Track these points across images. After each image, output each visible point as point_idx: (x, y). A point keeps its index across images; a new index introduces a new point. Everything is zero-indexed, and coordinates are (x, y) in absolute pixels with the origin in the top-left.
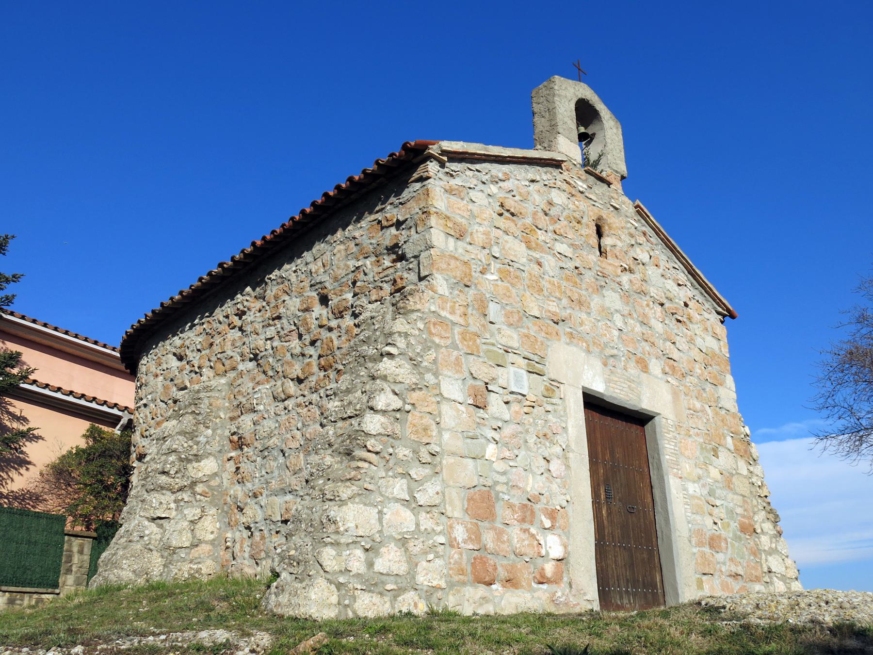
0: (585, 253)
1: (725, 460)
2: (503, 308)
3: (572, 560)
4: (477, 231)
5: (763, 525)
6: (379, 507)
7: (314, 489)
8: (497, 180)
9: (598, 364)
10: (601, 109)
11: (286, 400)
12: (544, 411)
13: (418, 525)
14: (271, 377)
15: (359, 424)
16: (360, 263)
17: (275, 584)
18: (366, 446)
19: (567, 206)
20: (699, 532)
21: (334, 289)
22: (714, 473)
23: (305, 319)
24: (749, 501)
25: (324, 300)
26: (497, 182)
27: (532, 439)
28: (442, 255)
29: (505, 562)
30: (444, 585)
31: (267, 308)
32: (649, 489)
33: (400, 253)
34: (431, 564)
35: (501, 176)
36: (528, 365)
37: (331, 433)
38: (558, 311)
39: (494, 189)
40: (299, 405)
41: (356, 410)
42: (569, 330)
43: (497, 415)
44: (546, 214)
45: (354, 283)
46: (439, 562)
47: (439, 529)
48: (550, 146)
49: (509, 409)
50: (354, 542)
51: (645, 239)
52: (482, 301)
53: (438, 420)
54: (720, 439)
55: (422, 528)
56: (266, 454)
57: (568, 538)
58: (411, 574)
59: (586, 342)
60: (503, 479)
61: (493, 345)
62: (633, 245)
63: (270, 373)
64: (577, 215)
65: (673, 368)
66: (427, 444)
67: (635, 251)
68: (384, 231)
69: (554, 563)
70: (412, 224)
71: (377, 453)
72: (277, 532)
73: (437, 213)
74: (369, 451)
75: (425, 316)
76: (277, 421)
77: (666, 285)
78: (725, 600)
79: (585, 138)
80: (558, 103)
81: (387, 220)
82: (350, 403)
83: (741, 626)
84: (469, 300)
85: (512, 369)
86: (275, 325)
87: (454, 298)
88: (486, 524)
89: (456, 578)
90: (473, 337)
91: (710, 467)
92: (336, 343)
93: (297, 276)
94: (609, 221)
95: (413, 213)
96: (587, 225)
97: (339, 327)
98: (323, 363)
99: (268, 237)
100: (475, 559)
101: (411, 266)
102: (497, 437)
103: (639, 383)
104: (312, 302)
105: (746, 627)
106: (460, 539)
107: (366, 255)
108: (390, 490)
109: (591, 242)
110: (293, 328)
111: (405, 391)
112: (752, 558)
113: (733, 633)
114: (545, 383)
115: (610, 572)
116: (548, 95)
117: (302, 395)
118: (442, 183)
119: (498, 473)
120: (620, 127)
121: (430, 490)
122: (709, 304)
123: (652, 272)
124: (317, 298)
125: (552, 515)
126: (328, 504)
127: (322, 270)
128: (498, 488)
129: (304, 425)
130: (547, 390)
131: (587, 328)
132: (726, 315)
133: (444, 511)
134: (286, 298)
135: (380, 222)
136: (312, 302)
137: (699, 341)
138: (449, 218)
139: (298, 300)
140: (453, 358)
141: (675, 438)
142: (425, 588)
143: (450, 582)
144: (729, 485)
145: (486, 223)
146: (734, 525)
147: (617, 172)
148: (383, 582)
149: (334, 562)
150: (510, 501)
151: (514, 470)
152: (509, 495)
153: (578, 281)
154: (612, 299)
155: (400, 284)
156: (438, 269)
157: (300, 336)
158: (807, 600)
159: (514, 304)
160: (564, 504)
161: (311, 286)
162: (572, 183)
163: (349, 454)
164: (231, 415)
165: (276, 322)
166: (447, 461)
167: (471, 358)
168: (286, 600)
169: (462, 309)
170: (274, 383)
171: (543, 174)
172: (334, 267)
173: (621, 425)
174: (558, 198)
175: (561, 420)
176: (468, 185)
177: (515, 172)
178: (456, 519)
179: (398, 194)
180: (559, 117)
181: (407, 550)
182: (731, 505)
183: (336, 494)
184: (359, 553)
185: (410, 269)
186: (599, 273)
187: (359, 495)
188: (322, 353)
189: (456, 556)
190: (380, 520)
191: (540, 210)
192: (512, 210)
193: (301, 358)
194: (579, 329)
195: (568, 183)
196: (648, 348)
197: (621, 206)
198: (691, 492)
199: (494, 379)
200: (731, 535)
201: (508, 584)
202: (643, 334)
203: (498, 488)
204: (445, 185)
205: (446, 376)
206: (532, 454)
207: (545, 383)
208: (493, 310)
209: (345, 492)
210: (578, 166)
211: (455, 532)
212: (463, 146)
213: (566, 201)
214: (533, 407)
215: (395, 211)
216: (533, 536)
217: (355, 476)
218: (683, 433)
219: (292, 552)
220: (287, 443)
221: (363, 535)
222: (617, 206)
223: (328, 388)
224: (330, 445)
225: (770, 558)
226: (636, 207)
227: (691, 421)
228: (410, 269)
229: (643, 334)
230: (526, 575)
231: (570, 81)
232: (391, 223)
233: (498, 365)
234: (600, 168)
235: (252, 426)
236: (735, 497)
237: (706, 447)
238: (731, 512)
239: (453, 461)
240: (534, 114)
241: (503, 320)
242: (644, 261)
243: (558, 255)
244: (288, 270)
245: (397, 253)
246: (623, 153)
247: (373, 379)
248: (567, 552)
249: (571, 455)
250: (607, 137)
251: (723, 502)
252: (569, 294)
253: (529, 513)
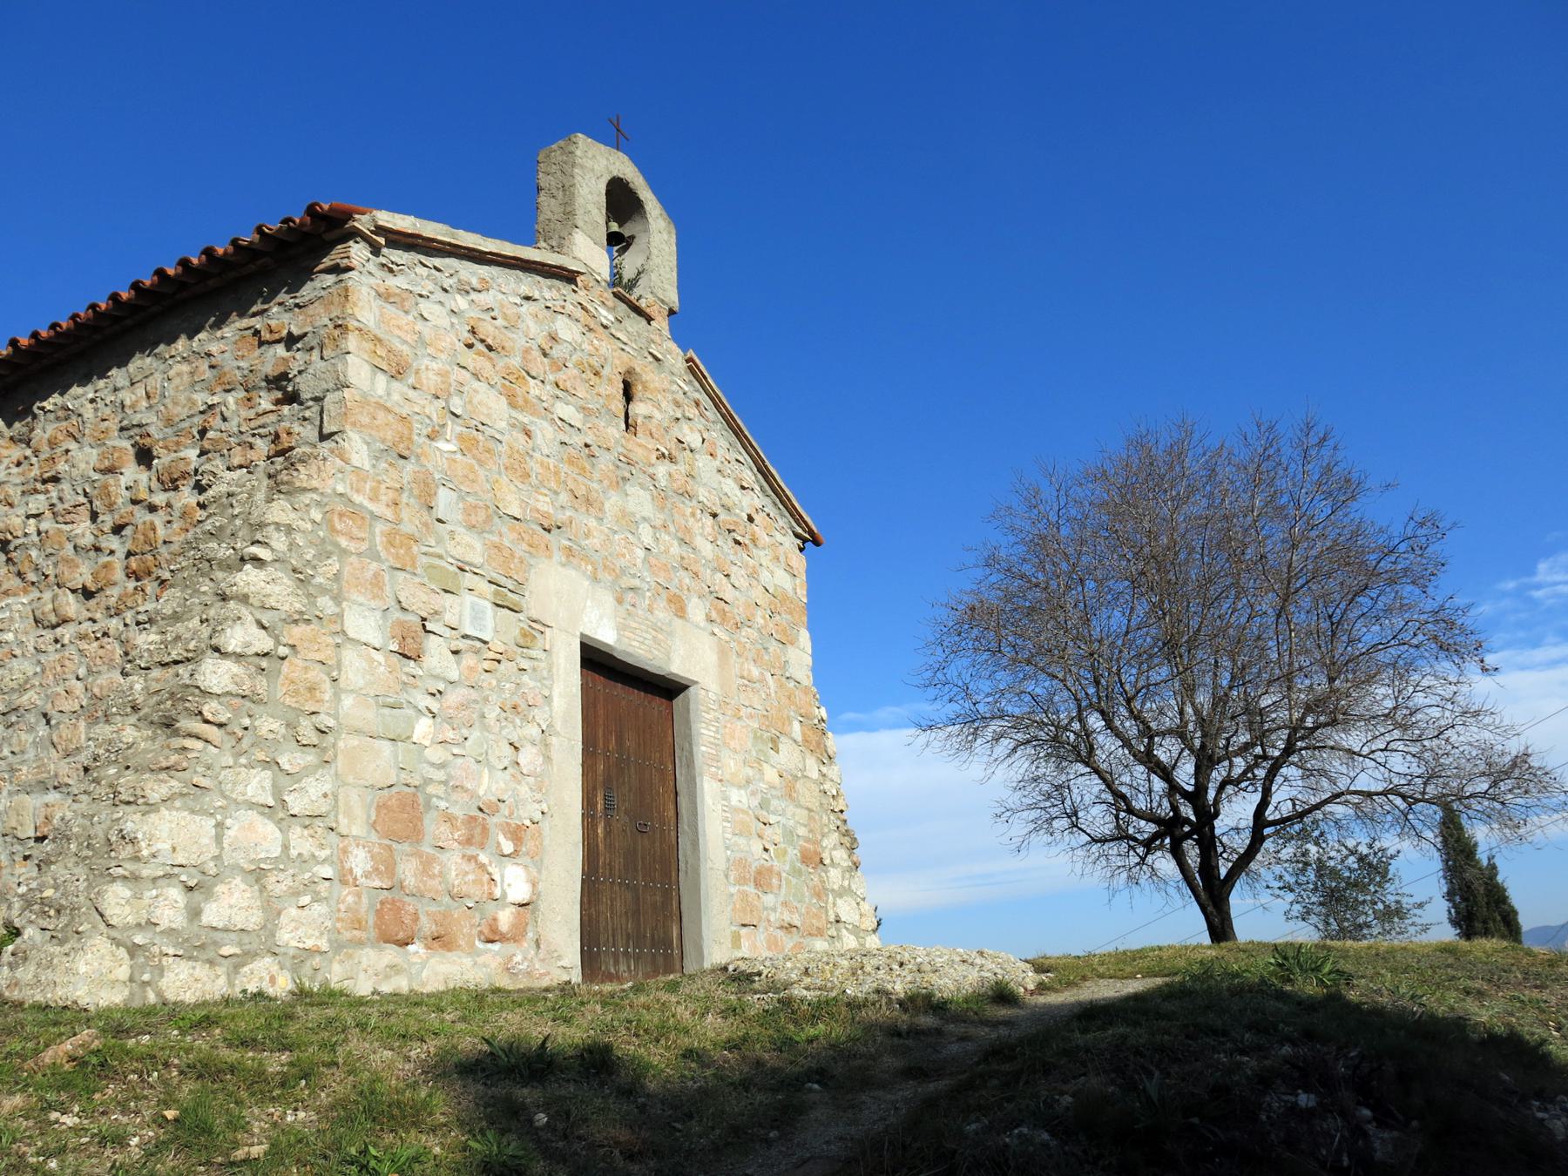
0: (603, 424)
1: (788, 755)
2: (461, 498)
3: (542, 906)
4: (427, 369)
5: (834, 853)
6: (219, 817)
7: (99, 783)
8: (468, 288)
9: (609, 599)
10: (646, 198)
11: (58, 625)
12: (515, 669)
13: (286, 847)
14: (33, 583)
15: (192, 675)
16: (216, 399)
17: (10, 948)
18: (200, 713)
19: (580, 346)
20: (742, 863)
21: (165, 439)
22: (771, 774)
23: (106, 487)
24: (817, 817)
25: (144, 456)
26: (468, 292)
27: (492, 714)
28: (364, 401)
29: (433, 908)
30: (324, 946)
31: (34, 460)
32: (672, 796)
33: (290, 389)
34: (306, 912)
35: (475, 282)
36: (496, 594)
37: (138, 687)
38: (551, 511)
39: (461, 302)
40: (82, 637)
41: (187, 651)
42: (567, 543)
43: (438, 671)
44: (545, 355)
45: (203, 432)
46: (318, 909)
47: (323, 854)
48: (560, 246)
49: (458, 663)
50: (167, 876)
51: (697, 412)
52: (427, 484)
53: (334, 674)
54: (784, 724)
55: (294, 853)
56: (14, 719)
57: (539, 871)
58: (269, 927)
59: (592, 564)
60: (440, 775)
61: (440, 557)
62: (678, 419)
63: (32, 577)
64: (595, 362)
65: (723, 613)
66: (313, 713)
67: (681, 429)
68: (263, 348)
69: (513, 909)
70: (314, 343)
71: (221, 725)
72: (26, 858)
73: (360, 330)
74: (207, 722)
75: (326, 500)
76: (39, 662)
77: (723, 485)
78: (763, 963)
79: (617, 242)
80: (579, 178)
81: (271, 332)
82: (178, 638)
83: (779, 1001)
84: (405, 481)
85: (468, 598)
86: (47, 492)
87: (378, 475)
88: (406, 847)
89: (347, 935)
90: (406, 541)
91: (765, 764)
92: (161, 533)
93: (96, 410)
94: (645, 377)
95: (318, 324)
96: (610, 380)
97: (169, 505)
98: (134, 565)
99: (44, 334)
100: (382, 903)
101: (307, 414)
102: (435, 707)
103: (671, 634)
104: (120, 458)
105: (787, 1003)
106: (358, 872)
107: (228, 387)
108: (240, 788)
109: (613, 407)
110: (82, 499)
111: (280, 624)
112: (815, 901)
113: (767, 1011)
114: (522, 625)
115: (602, 924)
116: (565, 163)
117: (90, 619)
118: (372, 281)
119: (433, 765)
120: (674, 231)
121: (312, 791)
122: (784, 521)
123: (703, 463)
124: (131, 451)
125: (516, 834)
126: (123, 808)
127: (145, 404)
128: (430, 789)
129: (90, 672)
130: (524, 635)
131: (595, 542)
132: (807, 540)
133: (334, 825)
134: (73, 446)
135: (257, 333)
136: (120, 458)
137: (765, 576)
138: (380, 340)
139: (95, 452)
140: (369, 574)
141: (717, 720)
142: (291, 952)
143: (336, 940)
144: (790, 793)
145: (443, 356)
146: (793, 853)
147: (663, 301)
148: (215, 943)
149: (127, 909)
150: (449, 811)
151: (460, 761)
152: (447, 801)
153: (588, 467)
154: (639, 500)
155: (285, 441)
156: (354, 424)
157: (94, 516)
158: (875, 962)
159: (481, 493)
160: (538, 816)
161: (122, 429)
162: (592, 309)
163: (168, 724)
165: (50, 486)
166: (346, 742)
167: (401, 575)
168: (30, 976)
169: (391, 494)
170: (38, 595)
171: (545, 289)
172: (167, 401)
173: (636, 696)
174: (567, 331)
175: (543, 685)
176: (418, 290)
177: (500, 280)
178: (356, 838)
179: (294, 288)
180: (579, 201)
181: (263, 888)
182: (791, 823)
183: (139, 793)
184: (175, 893)
186: (622, 458)
187: (182, 795)
188: (133, 548)
189: (350, 899)
190: (219, 839)
191: (535, 347)
192: (490, 341)
193: (92, 553)
194: (583, 543)
195: (584, 308)
196: (687, 581)
197: (665, 357)
198: (734, 802)
199: (436, 613)
200: (787, 868)
201: (435, 944)
202: (682, 558)
203: (430, 789)
204: (378, 285)
205: (355, 602)
206: (491, 736)
207: (522, 625)
208: (444, 500)
209: (156, 789)
210: (603, 284)
211: (352, 859)
212: (415, 225)
213: (579, 338)
214: (499, 662)
215: (286, 317)
216: (482, 867)
217: (177, 763)
218: (729, 712)
219: (49, 893)
220: (57, 702)
221: (184, 862)
222: (659, 356)
223: (141, 609)
224: (135, 709)
225: (839, 902)
226: (687, 361)
227: (742, 696)
228: (305, 419)
229: (682, 558)
230: (466, 927)
231: (602, 147)
232: (277, 336)
233: (446, 591)
234: (637, 292)
236: (798, 811)
237: (762, 735)
238: (789, 834)
239: (356, 743)
240: (539, 189)
241: (460, 517)
242: (693, 446)
243: (559, 423)
244: (78, 397)
245: (283, 388)
246: (675, 274)
247: (224, 600)
248: (535, 891)
249: (554, 740)
250: (653, 244)
251: (779, 818)
252: (571, 485)
253: (478, 830)
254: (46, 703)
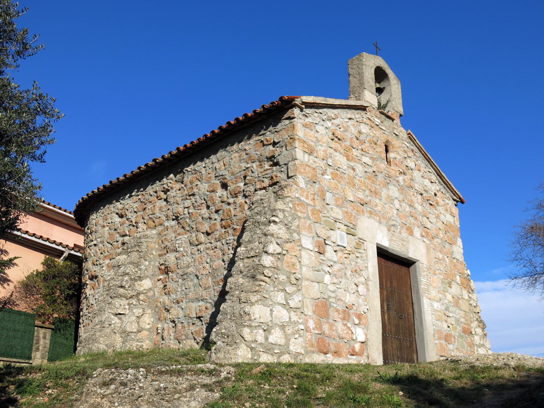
0: (379, 163)
1: (455, 289)
2: (334, 196)
3: (369, 343)
4: (320, 150)
5: (476, 329)
6: (271, 307)
7: (234, 296)
8: (331, 118)
9: (385, 229)
10: (389, 73)
11: (199, 245)
12: (355, 257)
13: (290, 318)
14: (188, 231)
15: (259, 261)
16: (249, 165)
17: (214, 348)
18: (263, 273)
19: (369, 134)
20: (439, 332)
21: (231, 180)
22: (449, 297)
23: (212, 197)
24: (468, 315)
25: (225, 186)
26: (331, 120)
27: (349, 273)
28: (302, 164)
29: (334, 342)
30: (303, 352)
31: (185, 188)
32: (411, 305)
33: (275, 161)
34: (297, 340)
35: (333, 116)
36: (347, 229)
37: (241, 265)
38: (363, 198)
39: (329, 124)
40: (208, 249)
41: (256, 253)
42: (369, 209)
43: (331, 258)
44: (357, 139)
45: (245, 177)
46: (301, 339)
47: (301, 321)
48: (359, 96)
49: (337, 255)
50: (259, 326)
51: (413, 154)
52: (322, 192)
53: (300, 260)
54: (453, 277)
55: (292, 320)
56: (186, 277)
57: (367, 331)
58: (287, 345)
59: (379, 217)
60: (333, 295)
61: (329, 217)
62: (406, 158)
63: (187, 228)
64: (374, 139)
65: (427, 233)
66: (294, 273)
67: (407, 162)
68: (265, 147)
69: (359, 344)
70: (283, 145)
71: (269, 277)
72: (193, 324)
73: (299, 139)
74: (265, 276)
75: (293, 200)
76: (193, 257)
77: (424, 182)
78: (461, 357)
79: (379, 91)
80: (365, 70)
81: (267, 141)
82: (252, 249)
83: (470, 367)
84: (316, 191)
85: (338, 232)
86: (191, 199)
87: (308, 190)
88: (324, 320)
89: (309, 349)
90: (317, 212)
91: (446, 293)
92: (233, 212)
93: (206, 170)
94: (393, 143)
95: (284, 138)
96: (380, 146)
97: (235, 203)
98: (224, 224)
99: (188, 145)
100: (319, 339)
101: (282, 169)
102: (330, 271)
103: (408, 242)
104: (216, 187)
105: (473, 367)
106: (311, 327)
107: (253, 161)
108: (276, 298)
109: (382, 156)
110: (203, 201)
111: (283, 243)
112: (469, 348)
113: (466, 370)
114: (356, 240)
115: (389, 352)
116: (359, 64)
117: (210, 243)
118: (301, 121)
119: (331, 291)
120: (400, 83)
121: (296, 299)
122: (449, 195)
123: (416, 174)
124: (220, 184)
125: (359, 317)
126: (243, 305)
127: (223, 168)
128: (331, 300)
129: (211, 260)
130: (357, 244)
131: (379, 208)
132: (459, 201)
133: (303, 311)
134: (199, 183)
135: (262, 141)
136: (216, 187)
137: (442, 217)
138: (305, 142)
139: (207, 185)
140: (307, 225)
141: (427, 275)
142: (294, 353)
143: (306, 351)
144: (457, 304)
145: (325, 145)
146: (459, 328)
147: (397, 112)
148: (273, 348)
149: (249, 336)
150: (337, 308)
151: (339, 290)
152: (336, 304)
153: (375, 180)
154: (394, 191)
155: (275, 180)
156: (299, 173)
157: (208, 207)
158: (502, 357)
159: (340, 193)
160: (366, 311)
161: (216, 177)
162: (372, 119)
163: (253, 277)
164: (160, 253)
165: (191, 197)
166: (305, 283)
167: (317, 225)
168: (222, 356)
169: (312, 196)
170: (190, 235)
171: (356, 114)
172: (231, 167)
173: (396, 266)
174: (364, 129)
175: (365, 262)
176: (315, 122)
177: (341, 114)
178: (310, 316)
179: (275, 125)
180: (365, 78)
181: (285, 331)
182: (458, 316)
183: (248, 299)
184: (261, 331)
185: (282, 171)
186: (386, 175)
187: (261, 300)
188: (223, 218)
189: (309, 337)
190: (271, 314)
191: (354, 137)
192: (339, 137)
193: (208, 220)
194: (375, 209)
195: (370, 119)
196: (413, 221)
197: (399, 134)
198: (435, 307)
199: (329, 237)
200: (457, 334)
201: (335, 355)
202: (411, 212)
203: (331, 300)
204: (303, 122)
205: (304, 235)
206: (349, 281)
207: (356, 240)
208: (328, 196)
209: (254, 298)
210: (376, 109)
211: (309, 323)
212: (314, 99)
213: (368, 131)
214: (349, 254)
215: (272, 136)
216: (349, 328)
217: (259, 290)
218: (432, 272)
219: (223, 331)
220: (200, 271)
221: (263, 322)
222: (397, 134)
223: (228, 239)
224: (241, 272)
225: (479, 349)
226: (408, 134)
227: (436, 265)
228: (282, 171)
229: (411, 212)
230: (345, 350)
231: (372, 56)
232: (269, 143)
233: (331, 229)
234: (387, 109)
235: (175, 260)
236: (461, 312)
237: (445, 281)
238: (457, 321)
239: (308, 283)
240: (349, 75)
241: (334, 203)
242: (412, 168)
243: (364, 164)
244: (200, 165)
245: (274, 162)
246: (401, 100)
247: (266, 236)
248: (366, 338)
249: (370, 283)
250: (392, 90)
251: (453, 314)
252: (370, 188)
253: (347, 315)
254: (197, 271)
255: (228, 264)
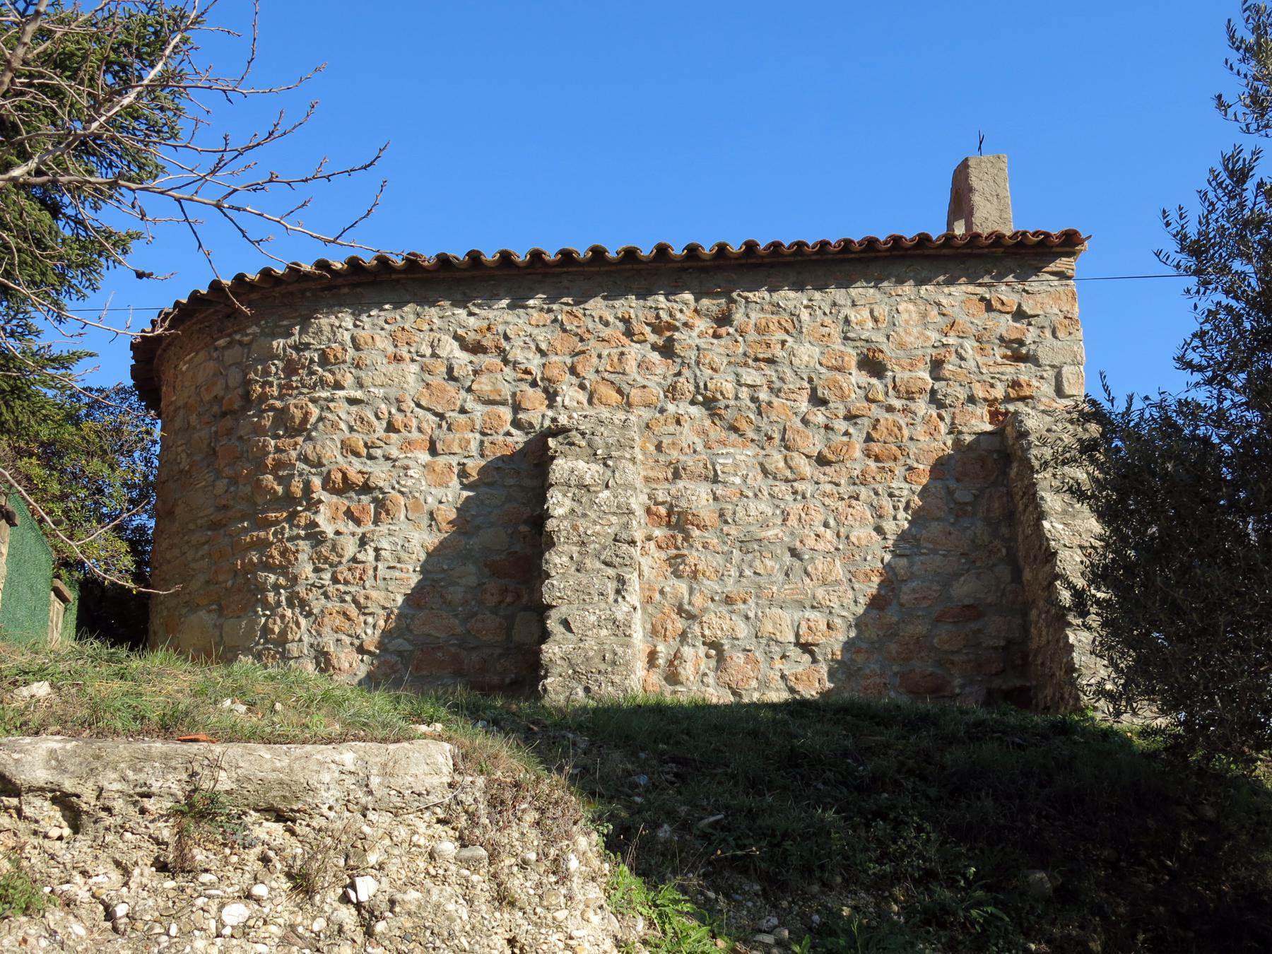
14: (752, 440)
107: (961, 334)
110: (806, 385)
164: (651, 474)
185: (1042, 377)
232: (1008, 309)
235: (711, 501)
254: (794, 540)
255: (896, 541)
